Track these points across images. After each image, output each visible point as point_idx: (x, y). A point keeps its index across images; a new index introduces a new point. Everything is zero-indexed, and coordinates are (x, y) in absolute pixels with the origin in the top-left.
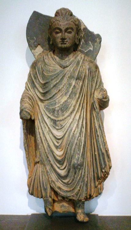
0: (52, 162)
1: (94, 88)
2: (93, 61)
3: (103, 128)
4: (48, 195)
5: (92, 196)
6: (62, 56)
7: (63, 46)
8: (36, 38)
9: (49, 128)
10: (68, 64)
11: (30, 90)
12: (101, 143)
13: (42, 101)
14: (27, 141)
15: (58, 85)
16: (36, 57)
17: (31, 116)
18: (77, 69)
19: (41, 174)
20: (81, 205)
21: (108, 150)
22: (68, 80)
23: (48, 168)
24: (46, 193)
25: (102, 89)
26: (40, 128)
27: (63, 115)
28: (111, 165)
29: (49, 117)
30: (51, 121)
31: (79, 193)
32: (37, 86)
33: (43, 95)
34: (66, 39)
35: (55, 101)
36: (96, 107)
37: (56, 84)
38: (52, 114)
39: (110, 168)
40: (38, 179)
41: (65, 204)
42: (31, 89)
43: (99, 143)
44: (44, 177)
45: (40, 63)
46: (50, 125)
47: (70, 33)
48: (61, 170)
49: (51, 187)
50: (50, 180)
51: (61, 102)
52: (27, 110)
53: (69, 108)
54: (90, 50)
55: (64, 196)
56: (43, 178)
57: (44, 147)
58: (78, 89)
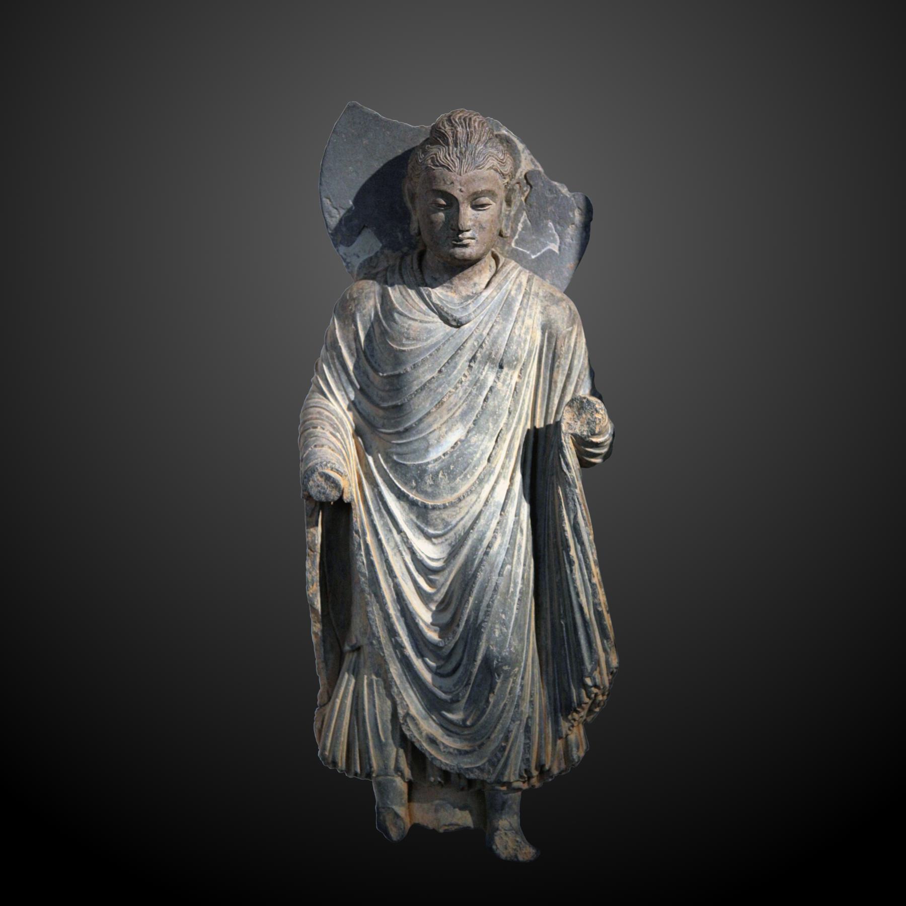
12: (581, 589)
17: (342, 492)
27: (453, 490)
53: (474, 467)
55: (448, 769)
56: (374, 706)
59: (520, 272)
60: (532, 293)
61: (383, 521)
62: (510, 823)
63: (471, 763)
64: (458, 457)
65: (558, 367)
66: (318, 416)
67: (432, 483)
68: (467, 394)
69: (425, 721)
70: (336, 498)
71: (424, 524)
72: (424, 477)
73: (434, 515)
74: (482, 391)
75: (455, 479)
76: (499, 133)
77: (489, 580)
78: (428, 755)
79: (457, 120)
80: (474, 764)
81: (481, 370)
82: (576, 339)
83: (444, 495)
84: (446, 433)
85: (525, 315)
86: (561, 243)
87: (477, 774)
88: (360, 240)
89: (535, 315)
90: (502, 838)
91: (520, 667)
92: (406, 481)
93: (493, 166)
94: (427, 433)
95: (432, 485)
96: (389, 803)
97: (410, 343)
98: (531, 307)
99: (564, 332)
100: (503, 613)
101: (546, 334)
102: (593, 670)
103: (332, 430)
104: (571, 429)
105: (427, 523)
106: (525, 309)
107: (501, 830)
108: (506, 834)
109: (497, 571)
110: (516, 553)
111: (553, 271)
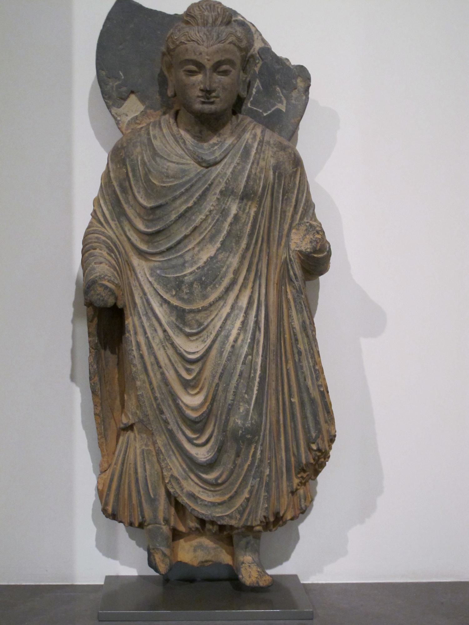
0: (173, 426)
1: (288, 220)
2: (286, 143)
3: (314, 330)
4: (161, 516)
5: (282, 517)
6: (201, 132)
7: (207, 108)
8: (124, 76)
9: (165, 331)
10: (218, 155)
11: (107, 222)
12: (308, 373)
13: (142, 254)
14: (98, 367)
15: (190, 213)
16: (124, 126)
17: (116, 298)
18: (243, 169)
19: (139, 459)
20: (252, 542)
21: (328, 392)
22: (218, 199)
23: (161, 440)
24: (155, 510)
25: (311, 225)
26: (139, 330)
27: (205, 297)
28: (333, 433)
29: (165, 301)
30: (171, 313)
31: (247, 506)
32: (130, 212)
33: (147, 238)
34: (214, 91)
35: (181, 256)
36: (295, 275)
37: (186, 211)
38: (174, 293)
39: (332, 440)
40: (132, 472)
41: (206, 541)
42: (110, 221)
43: (303, 373)
44: (148, 467)
45: (138, 149)
46: (168, 323)
47: (225, 73)
48: (198, 446)
49: (168, 493)
50: (165, 473)
51: (199, 259)
52: (106, 283)
53: (221, 278)
54: (279, 111)
57: (151, 383)
58: (245, 224)
59: (255, 126)
60: (265, 141)
61: (149, 323)
62: (252, 558)
63: (221, 513)
64: (208, 270)
65: (286, 199)
66: (96, 240)
67: (188, 291)
68: (215, 221)
69: (186, 481)
70: (113, 304)
71: (182, 325)
72: (182, 286)
73: (189, 317)
74: (227, 218)
75: (206, 288)
76: (236, 19)
77: (234, 368)
78: (188, 507)
79: (204, 7)
80: (224, 513)
81: (226, 201)
82: (300, 177)
83: (197, 301)
84: (199, 251)
85: (259, 158)
86: (286, 104)
87: (226, 521)
88: (128, 103)
89: (267, 159)
90: (246, 569)
91: (260, 435)
92: (167, 290)
93: (232, 41)
94: (183, 252)
95: (188, 293)
96: (158, 545)
97: (168, 180)
98: (264, 152)
99: (290, 172)
100: (245, 393)
101: (277, 174)
102: (317, 437)
103: (107, 251)
104: (298, 247)
105: (185, 324)
106: (259, 154)
107: (246, 564)
108: (249, 566)
109: (242, 360)
110: (255, 346)
111: (281, 126)
